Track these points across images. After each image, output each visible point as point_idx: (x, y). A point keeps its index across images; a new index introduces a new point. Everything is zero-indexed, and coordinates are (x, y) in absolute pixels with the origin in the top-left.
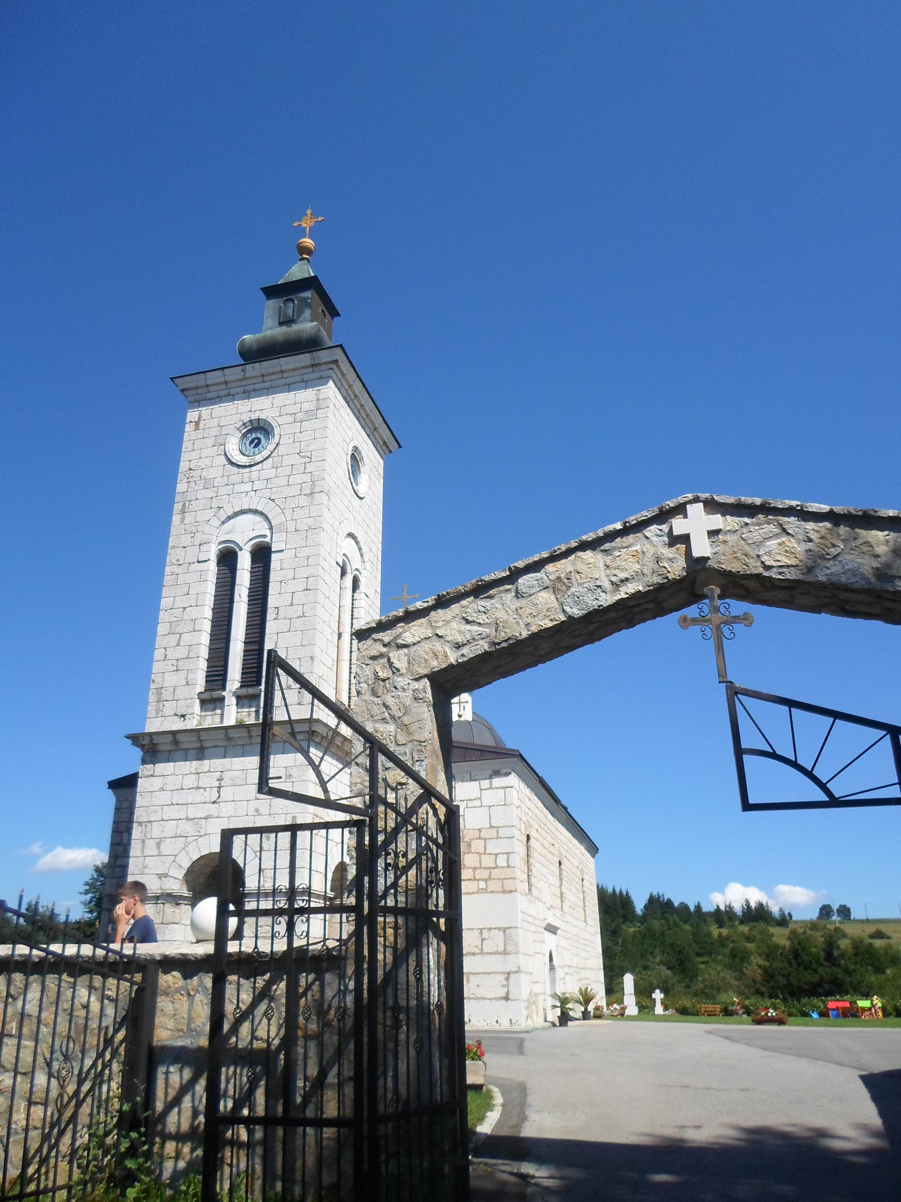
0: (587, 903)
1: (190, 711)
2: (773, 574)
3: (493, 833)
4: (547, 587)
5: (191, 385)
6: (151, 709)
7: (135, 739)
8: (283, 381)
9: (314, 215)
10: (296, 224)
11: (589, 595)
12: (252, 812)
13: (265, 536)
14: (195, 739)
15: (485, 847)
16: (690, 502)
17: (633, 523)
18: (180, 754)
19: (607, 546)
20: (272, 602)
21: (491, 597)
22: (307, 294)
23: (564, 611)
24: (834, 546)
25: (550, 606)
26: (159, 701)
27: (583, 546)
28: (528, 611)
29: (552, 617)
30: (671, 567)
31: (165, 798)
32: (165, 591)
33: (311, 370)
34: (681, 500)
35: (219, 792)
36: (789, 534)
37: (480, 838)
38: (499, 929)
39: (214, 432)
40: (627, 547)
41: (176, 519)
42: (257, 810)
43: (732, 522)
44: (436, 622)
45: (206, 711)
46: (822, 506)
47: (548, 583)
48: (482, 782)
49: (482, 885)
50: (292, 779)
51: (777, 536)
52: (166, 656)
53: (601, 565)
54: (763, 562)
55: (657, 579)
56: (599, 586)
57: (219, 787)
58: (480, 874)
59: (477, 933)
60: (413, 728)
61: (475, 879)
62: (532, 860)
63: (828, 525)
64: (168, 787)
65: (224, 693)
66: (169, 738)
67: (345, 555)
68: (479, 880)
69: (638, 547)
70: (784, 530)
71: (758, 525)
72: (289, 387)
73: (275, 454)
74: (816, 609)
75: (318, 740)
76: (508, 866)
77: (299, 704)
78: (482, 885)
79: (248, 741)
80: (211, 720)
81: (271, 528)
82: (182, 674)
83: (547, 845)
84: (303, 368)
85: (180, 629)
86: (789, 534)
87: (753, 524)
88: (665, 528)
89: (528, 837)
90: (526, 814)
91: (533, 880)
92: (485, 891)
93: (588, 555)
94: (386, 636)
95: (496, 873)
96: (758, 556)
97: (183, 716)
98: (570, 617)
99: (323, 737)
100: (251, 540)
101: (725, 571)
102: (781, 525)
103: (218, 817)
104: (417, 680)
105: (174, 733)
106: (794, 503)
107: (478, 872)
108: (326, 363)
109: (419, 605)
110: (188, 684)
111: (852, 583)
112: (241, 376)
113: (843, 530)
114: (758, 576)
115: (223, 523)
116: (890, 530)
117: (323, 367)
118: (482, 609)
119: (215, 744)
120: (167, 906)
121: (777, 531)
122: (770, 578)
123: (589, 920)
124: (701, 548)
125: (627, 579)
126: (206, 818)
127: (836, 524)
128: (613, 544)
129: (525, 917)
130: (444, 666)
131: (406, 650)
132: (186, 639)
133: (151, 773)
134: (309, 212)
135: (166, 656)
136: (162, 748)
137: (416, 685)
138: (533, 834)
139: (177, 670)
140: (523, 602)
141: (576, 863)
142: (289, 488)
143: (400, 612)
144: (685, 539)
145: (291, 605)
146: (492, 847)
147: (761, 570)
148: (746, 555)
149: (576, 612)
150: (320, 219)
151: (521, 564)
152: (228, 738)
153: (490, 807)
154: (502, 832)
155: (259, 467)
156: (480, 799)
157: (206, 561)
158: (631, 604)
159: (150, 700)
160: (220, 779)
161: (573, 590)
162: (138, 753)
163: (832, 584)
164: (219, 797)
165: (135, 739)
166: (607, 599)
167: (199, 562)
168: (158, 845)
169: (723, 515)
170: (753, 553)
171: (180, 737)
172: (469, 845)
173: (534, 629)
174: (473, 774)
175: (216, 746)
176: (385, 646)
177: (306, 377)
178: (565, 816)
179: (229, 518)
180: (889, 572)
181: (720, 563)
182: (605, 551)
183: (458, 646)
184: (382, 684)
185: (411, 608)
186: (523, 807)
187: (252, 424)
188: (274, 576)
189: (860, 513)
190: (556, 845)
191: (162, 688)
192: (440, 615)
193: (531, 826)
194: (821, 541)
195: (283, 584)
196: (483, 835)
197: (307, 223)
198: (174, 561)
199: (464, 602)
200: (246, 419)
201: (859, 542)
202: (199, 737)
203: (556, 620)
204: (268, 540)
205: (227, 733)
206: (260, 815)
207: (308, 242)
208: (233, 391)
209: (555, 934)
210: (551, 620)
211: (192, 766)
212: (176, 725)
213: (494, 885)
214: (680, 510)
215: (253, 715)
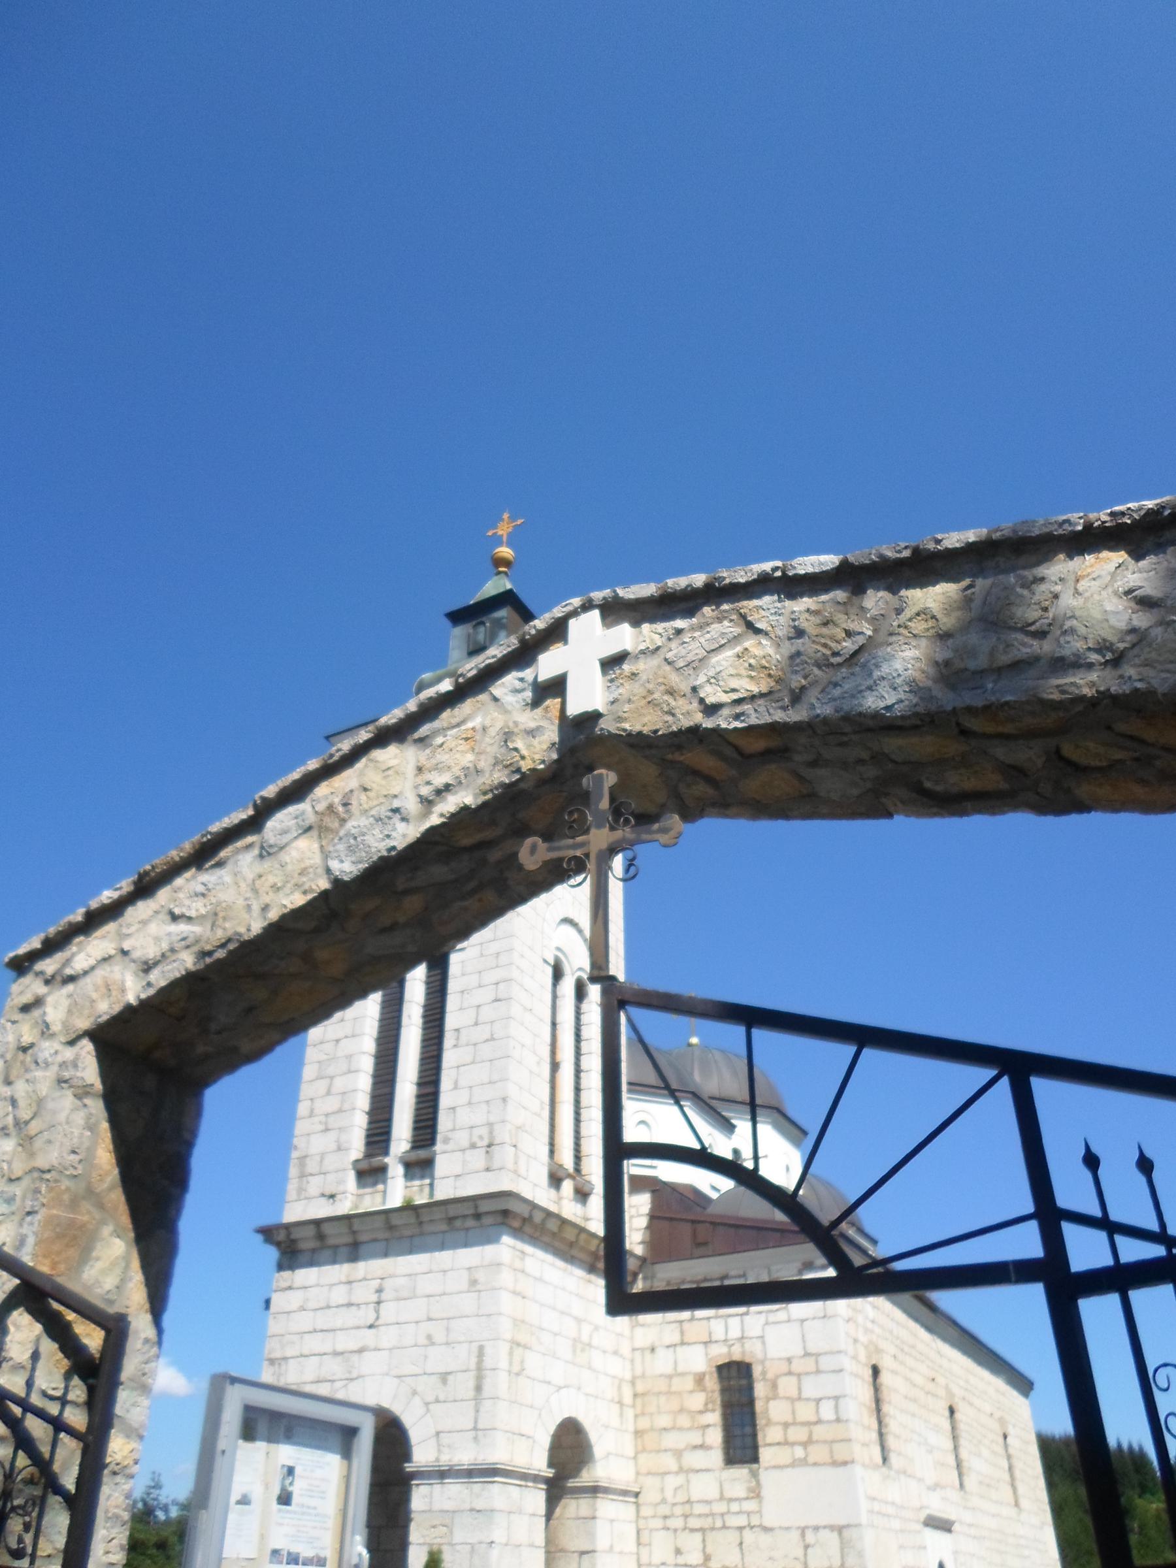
0: (1017, 1474)
1: (341, 1188)
2: (724, 721)
3: (810, 1364)
4: (310, 828)
6: (292, 1187)
7: (268, 1233)
9: (512, 518)
10: (490, 533)
11: (376, 832)
12: (422, 1340)
14: (344, 1230)
15: (800, 1389)
16: (574, 613)
17: (470, 675)
18: (327, 1253)
19: (424, 730)
20: (453, 1019)
21: (220, 864)
22: (503, 613)
23: (328, 871)
24: (849, 634)
25: (308, 863)
27: (383, 738)
28: (271, 879)
29: (306, 887)
30: (529, 746)
31: (304, 1321)
34: (558, 612)
35: (377, 1311)
36: (758, 631)
37: (790, 1373)
38: (832, 1528)
40: (458, 725)
42: (429, 1337)
43: (652, 633)
44: (129, 925)
46: (824, 558)
47: (311, 818)
49: (799, 1452)
50: (479, 1287)
51: (736, 639)
53: (410, 770)
54: (702, 701)
55: (502, 777)
56: (396, 811)
57: (378, 1303)
59: (795, 1535)
60: (38, 1143)
62: (886, 1408)
63: (840, 595)
64: (312, 1305)
65: (387, 1160)
66: (310, 1231)
67: (558, 949)
68: (793, 1444)
69: (477, 722)
70: (750, 626)
71: (701, 627)
74: (872, 805)
75: (516, 1224)
76: (838, 1420)
77: (488, 1170)
78: (799, 1452)
80: (371, 1201)
82: (332, 1136)
83: (920, 1380)
85: (331, 1071)
86: (758, 631)
87: (692, 629)
88: (528, 674)
89: (876, 1371)
90: (867, 1331)
91: (891, 1442)
92: (803, 1462)
93: (389, 755)
94: (48, 966)
95: (819, 1432)
96: (694, 689)
97: (332, 1196)
98: (337, 882)
99: (524, 1220)
101: (630, 735)
102: (743, 617)
104: (72, 1043)
105: (317, 1223)
106: (767, 566)
109: (107, 896)
111: (888, 708)
113: (875, 600)
114: (694, 732)
116: (974, 576)
118: (200, 889)
121: (737, 630)
122: (716, 731)
123: (1024, 1503)
124: (588, 694)
125: (447, 788)
126: (360, 1351)
127: (858, 590)
128: (436, 724)
129: (876, 1507)
130: (117, 1009)
131: (70, 987)
132: (339, 1084)
134: (506, 516)
136: (303, 1245)
137: (68, 1053)
138: (886, 1363)
139: (327, 1130)
140: (267, 864)
141: (988, 1408)
143: (78, 916)
144: (557, 687)
145: (476, 1024)
146: (811, 1388)
147: (698, 718)
148: (671, 692)
149: (347, 868)
150: (519, 522)
151: (270, 791)
152: (391, 1228)
153: (803, 1321)
154: (825, 1363)
158: (466, 841)
160: (379, 1291)
161: (350, 825)
162: (272, 1253)
163: (847, 718)
164: (377, 1318)
165: (268, 1233)
166: (405, 834)
169: (636, 624)
170: (685, 687)
171: (327, 1229)
172: (774, 1386)
173: (273, 915)
174: (773, 1268)
175: (375, 1240)
176: (47, 982)
178: (952, 1331)
180: (972, 665)
181: (620, 719)
182: (421, 740)
183: (147, 967)
184: (21, 1055)
185: (94, 904)
186: (860, 1319)
188: (453, 986)
189: (906, 554)
190: (941, 1380)
191: (306, 1157)
192: (142, 909)
193: (878, 1351)
194: (825, 631)
195: (466, 996)
196: (797, 1367)
197: (503, 530)
199: (179, 881)
201: (908, 613)
202: (350, 1226)
203: (311, 890)
205: (388, 1221)
206: (433, 1344)
207: (505, 551)
209: (949, 1531)
210: (305, 893)
211: (340, 1271)
212: (322, 1210)
213: (818, 1453)
214: (557, 632)
215: (427, 1190)
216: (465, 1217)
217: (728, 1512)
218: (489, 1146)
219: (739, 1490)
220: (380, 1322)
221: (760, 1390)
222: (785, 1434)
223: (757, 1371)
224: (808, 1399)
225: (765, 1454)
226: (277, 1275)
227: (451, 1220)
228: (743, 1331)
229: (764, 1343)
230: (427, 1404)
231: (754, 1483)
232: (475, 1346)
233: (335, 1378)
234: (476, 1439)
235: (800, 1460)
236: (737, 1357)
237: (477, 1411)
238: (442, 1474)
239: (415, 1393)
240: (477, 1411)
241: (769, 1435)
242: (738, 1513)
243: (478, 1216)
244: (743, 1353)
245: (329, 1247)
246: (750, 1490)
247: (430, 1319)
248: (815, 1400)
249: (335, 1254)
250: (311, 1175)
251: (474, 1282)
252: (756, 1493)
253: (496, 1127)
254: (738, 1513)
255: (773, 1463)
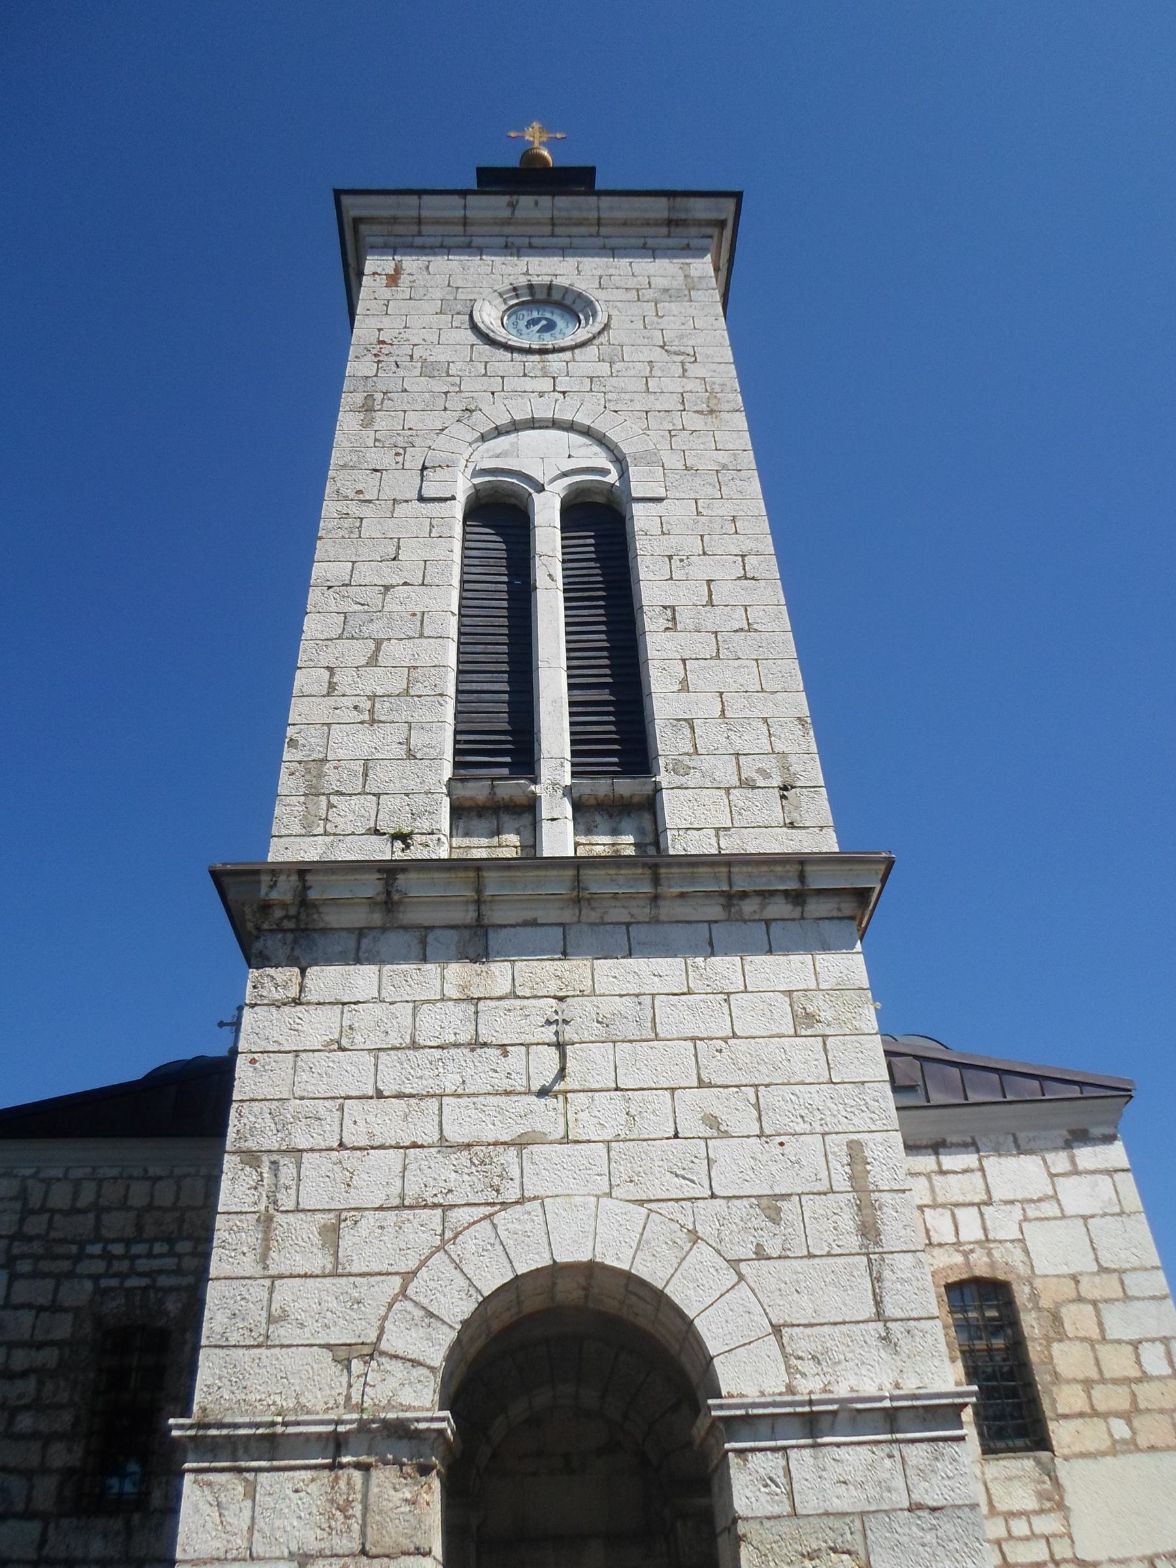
1: (425, 824)
3: (1109, 1287)
5: (384, 213)
8: (600, 241)
10: (512, 134)
12: (691, 1125)
13: (605, 472)
15: (1100, 1324)
18: (394, 939)
26: (313, 792)
31: (353, 1074)
32: (322, 549)
33: (664, 230)
37: (1080, 1299)
39: (438, 294)
41: (347, 421)
45: (467, 834)
48: (1050, 1157)
49: (1120, 1429)
50: (819, 1029)
52: (332, 687)
58: (1104, 1397)
61: (1095, 1413)
66: (371, 887)
72: (613, 252)
73: (603, 339)
77: (792, 825)
79: (643, 912)
81: (620, 460)
84: (647, 223)
85: (376, 629)
92: (1131, 1446)
97: (403, 838)
100: (565, 474)
103: (566, 1140)
107: (1098, 1392)
108: (700, 223)
110: (411, 755)
112: (506, 213)
115: (483, 438)
117: (693, 231)
119: (528, 915)
120: (383, 1477)
126: (520, 1144)
132: (395, 652)
133: (293, 992)
135: (332, 687)
136: (333, 918)
139: (373, 721)
142: (652, 397)
150: (558, 136)
153: (1085, 1218)
155: (567, 355)
156: (1055, 1197)
157: (446, 499)
159: (281, 790)
164: (562, 1074)
167: (421, 499)
168: (331, 1235)
172: (1056, 1319)
174: (1022, 1136)
175: (533, 923)
177: (651, 242)
179: (499, 432)
187: (532, 294)
191: (324, 760)
196: (1088, 1288)
198: (352, 495)
200: (522, 281)
204: (613, 478)
205: (577, 882)
206: (727, 1135)
208: (477, 241)
216: (766, 895)
217: (1010, 1537)
218: (785, 788)
219: (1023, 1497)
220: (569, 1083)
221: (1031, 1324)
222: (1090, 1398)
223: (1021, 1294)
224: (1119, 1342)
225: (1060, 1433)
226: (254, 973)
227: (731, 899)
228: (985, 1229)
229: (1026, 1251)
230: (734, 1263)
231: (1048, 1485)
232: (838, 1144)
233: (450, 1199)
234: (886, 1339)
235: (1124, 1441)
236: (981, 1271)
237: (877, 1279)
238: (812, 1423)
239: (694, 1237)
240: (877, 1279)
241: (1061, 1400)
242: (1027, 1539)
243: (798, 897)
244: (992, 1265)
245: (405, 928)
246: (1041, 1496)
247: (701, 1084)
248: (1130, 1343)
249: (423, 943)
250: (339, 793)
251: (805, 1020)
252: (1054, 1499)
253: (793, 759)
254: (1027, 1539)
255: (1077, 1448)
